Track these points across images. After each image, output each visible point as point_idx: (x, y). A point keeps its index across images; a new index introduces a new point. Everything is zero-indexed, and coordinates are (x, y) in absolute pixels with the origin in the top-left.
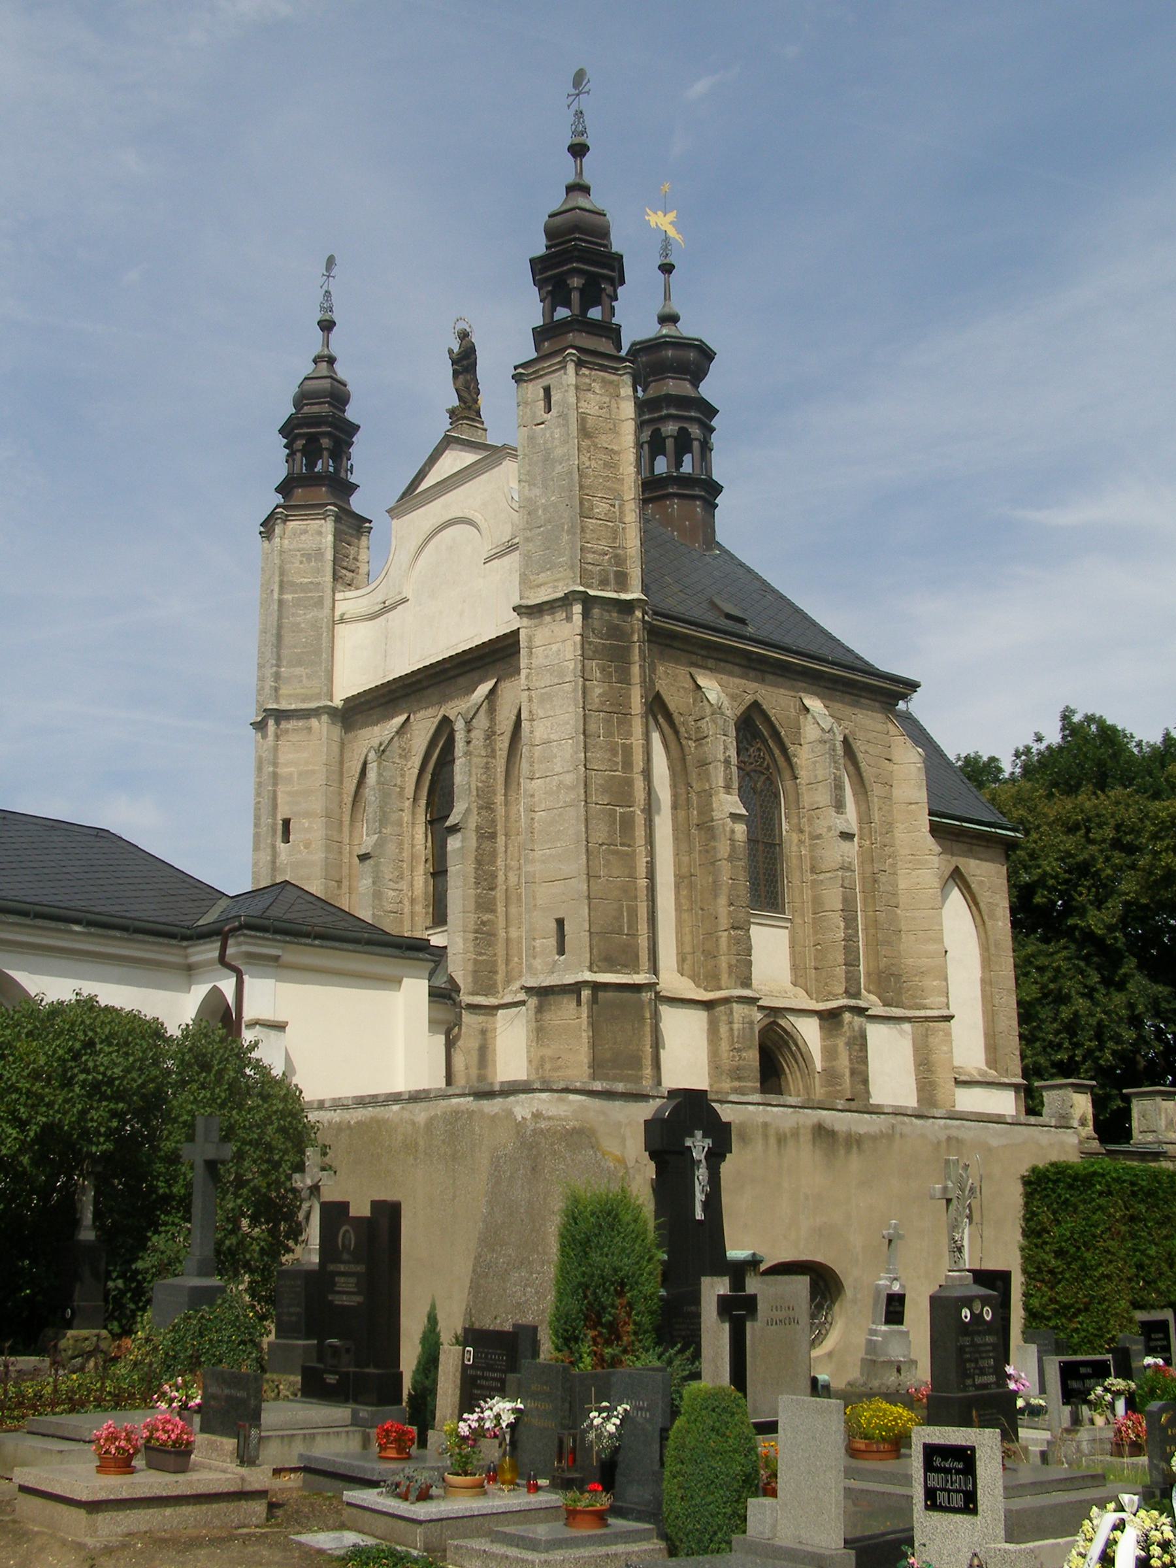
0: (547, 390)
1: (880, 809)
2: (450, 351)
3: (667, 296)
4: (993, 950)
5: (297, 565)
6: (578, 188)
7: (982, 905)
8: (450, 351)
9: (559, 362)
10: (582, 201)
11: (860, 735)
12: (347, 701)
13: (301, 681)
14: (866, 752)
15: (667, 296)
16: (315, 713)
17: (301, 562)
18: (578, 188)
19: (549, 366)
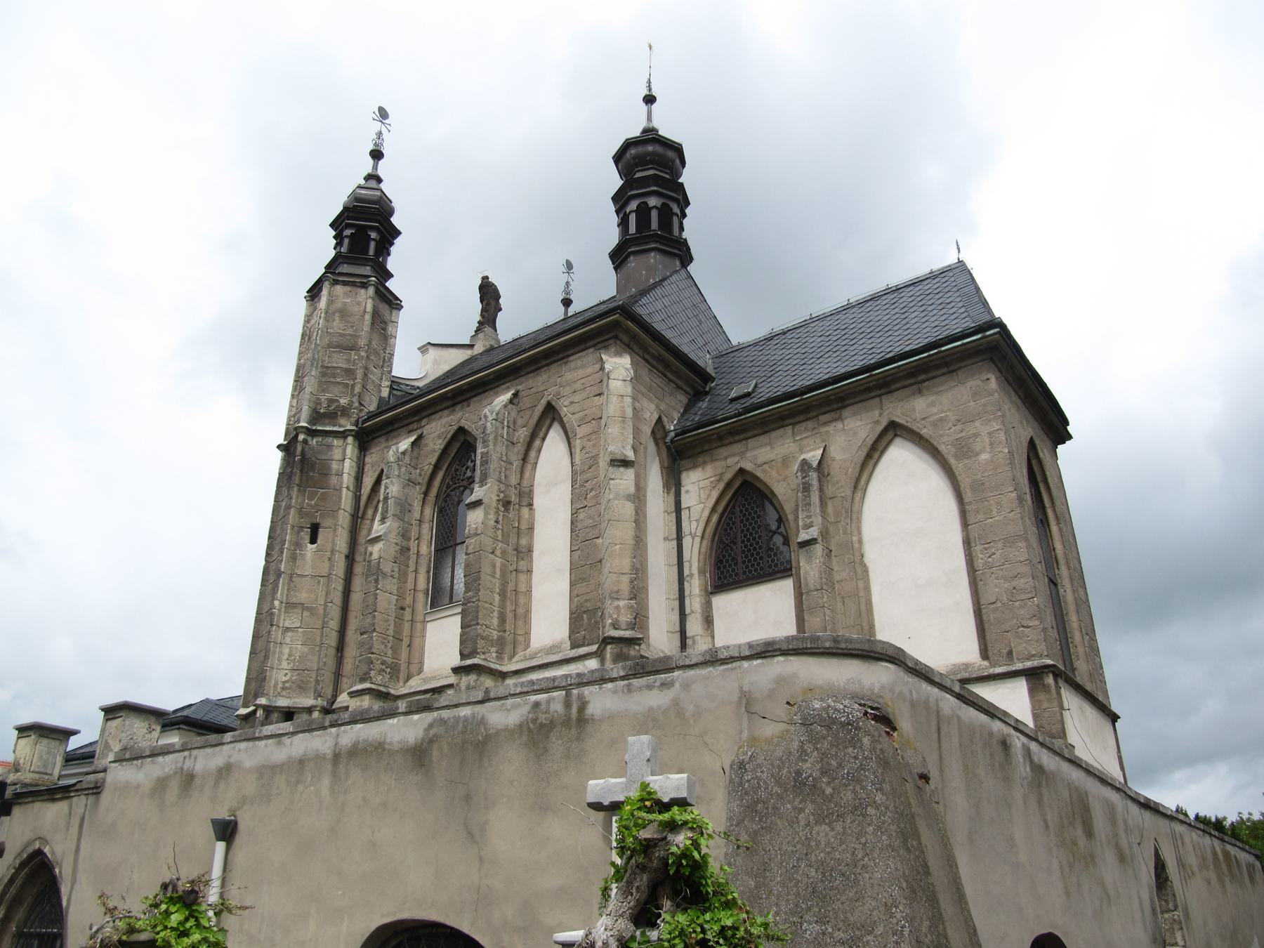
1: (583, 448)
3: (649, 118)
4: (968, 496)
6: (374, 178)
7: (942, 448)
10: (373, 184)
11: (566, 391)
14: (572, 403)
15: (649, 118)
18: (374, 178)
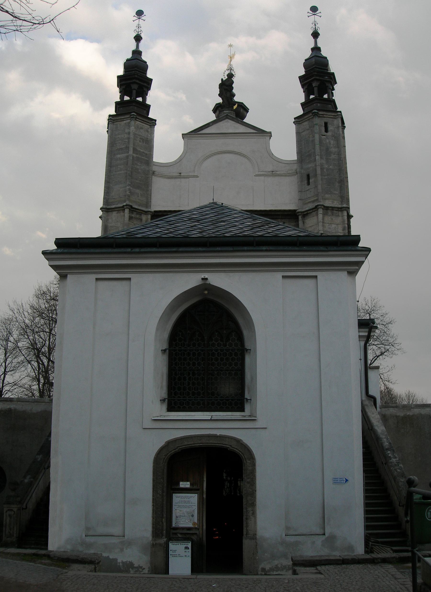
0: (326, 124)
2: (222, 79)
5: (138, 142)
6: (316, 49)
8: (222, 79)
9: (334, 116)
12: (155, 211)
13: (138, 196)
16: (146, 213)
17: (140, 141)
18: (316, 49)
19: (329, 115)
